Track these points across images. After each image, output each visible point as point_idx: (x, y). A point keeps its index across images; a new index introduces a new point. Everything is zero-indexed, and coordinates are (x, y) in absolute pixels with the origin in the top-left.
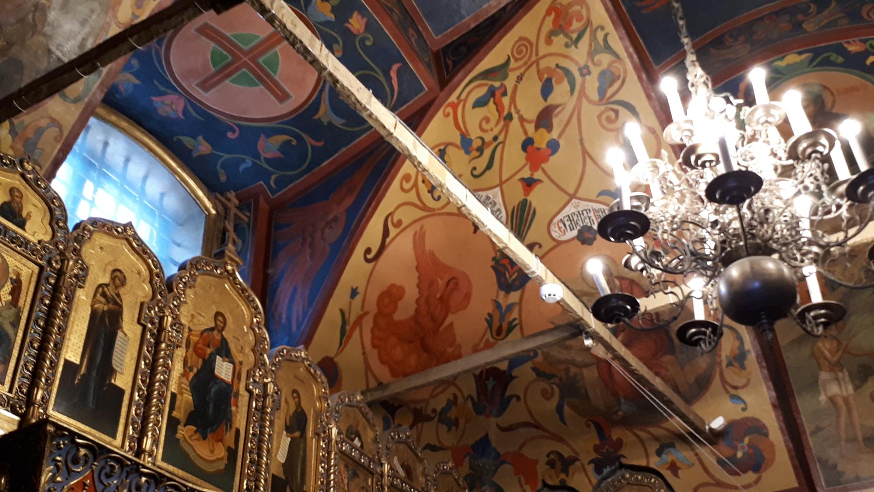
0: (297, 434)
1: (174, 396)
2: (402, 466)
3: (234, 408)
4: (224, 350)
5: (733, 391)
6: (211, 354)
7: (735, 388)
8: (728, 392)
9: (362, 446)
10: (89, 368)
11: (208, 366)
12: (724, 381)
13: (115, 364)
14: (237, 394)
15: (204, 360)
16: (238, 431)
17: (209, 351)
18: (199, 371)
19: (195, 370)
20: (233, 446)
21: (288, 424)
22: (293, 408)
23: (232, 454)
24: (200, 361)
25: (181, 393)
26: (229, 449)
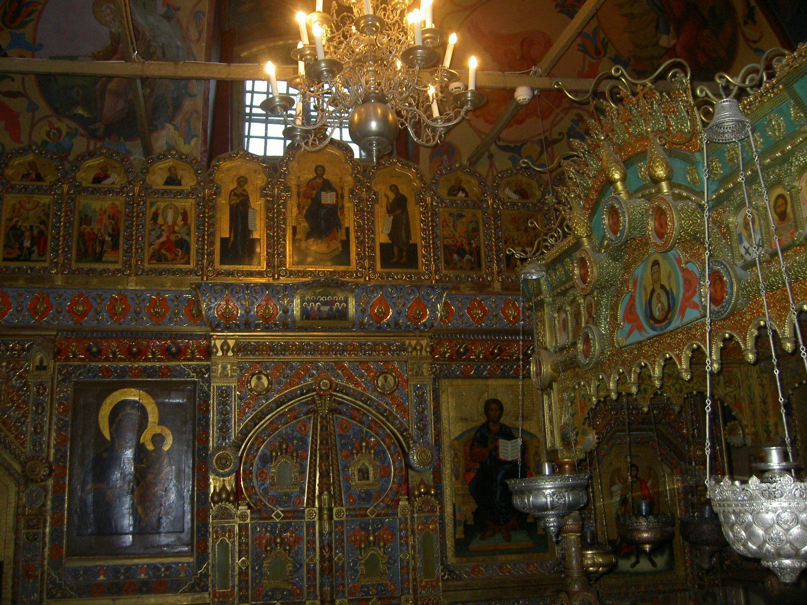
0: (399, 212)
1: (294, 229)
2: (515, 192)
3: (341, 217)
4: (327, 186)
5: (755, 46)
6: (317, 193)
7: (755, 42)
8: (752, 48)
9: (467, 195)
10: (235, 236)
11: (316, 201)
12: (746, 40)
13: (250, 228)
14: (343, 207)
15: (313, 200)
16: (347, 229)
17: (314, 192)
18: (309, 207)
19: (307, 207)
20: (344, 238)
21: (389, 208)
22: (392, 196)
23: (346, 244)
24: (309, 201)
25: (300, 224)
26: (342, 242)
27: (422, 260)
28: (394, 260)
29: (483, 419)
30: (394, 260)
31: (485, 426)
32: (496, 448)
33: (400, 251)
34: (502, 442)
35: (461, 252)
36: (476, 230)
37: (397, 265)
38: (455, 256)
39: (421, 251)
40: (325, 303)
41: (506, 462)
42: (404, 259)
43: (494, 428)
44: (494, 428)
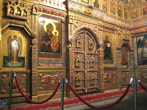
27: (100, 7)
28: (96, 6)
29: (105, 39)
30: (96, 6)
31: (106, 40)
32: (107, 45)
33: (97, 5)
34: (108, 43)
35: (105, 8)
36: (106, 4)
37: (96, 7)
38: (104, 8)
39: (100, 5)
40: (89, 11)
41: (109, 47)
42: (97, 6)
43: (107, 41)
44: (107, 41)
